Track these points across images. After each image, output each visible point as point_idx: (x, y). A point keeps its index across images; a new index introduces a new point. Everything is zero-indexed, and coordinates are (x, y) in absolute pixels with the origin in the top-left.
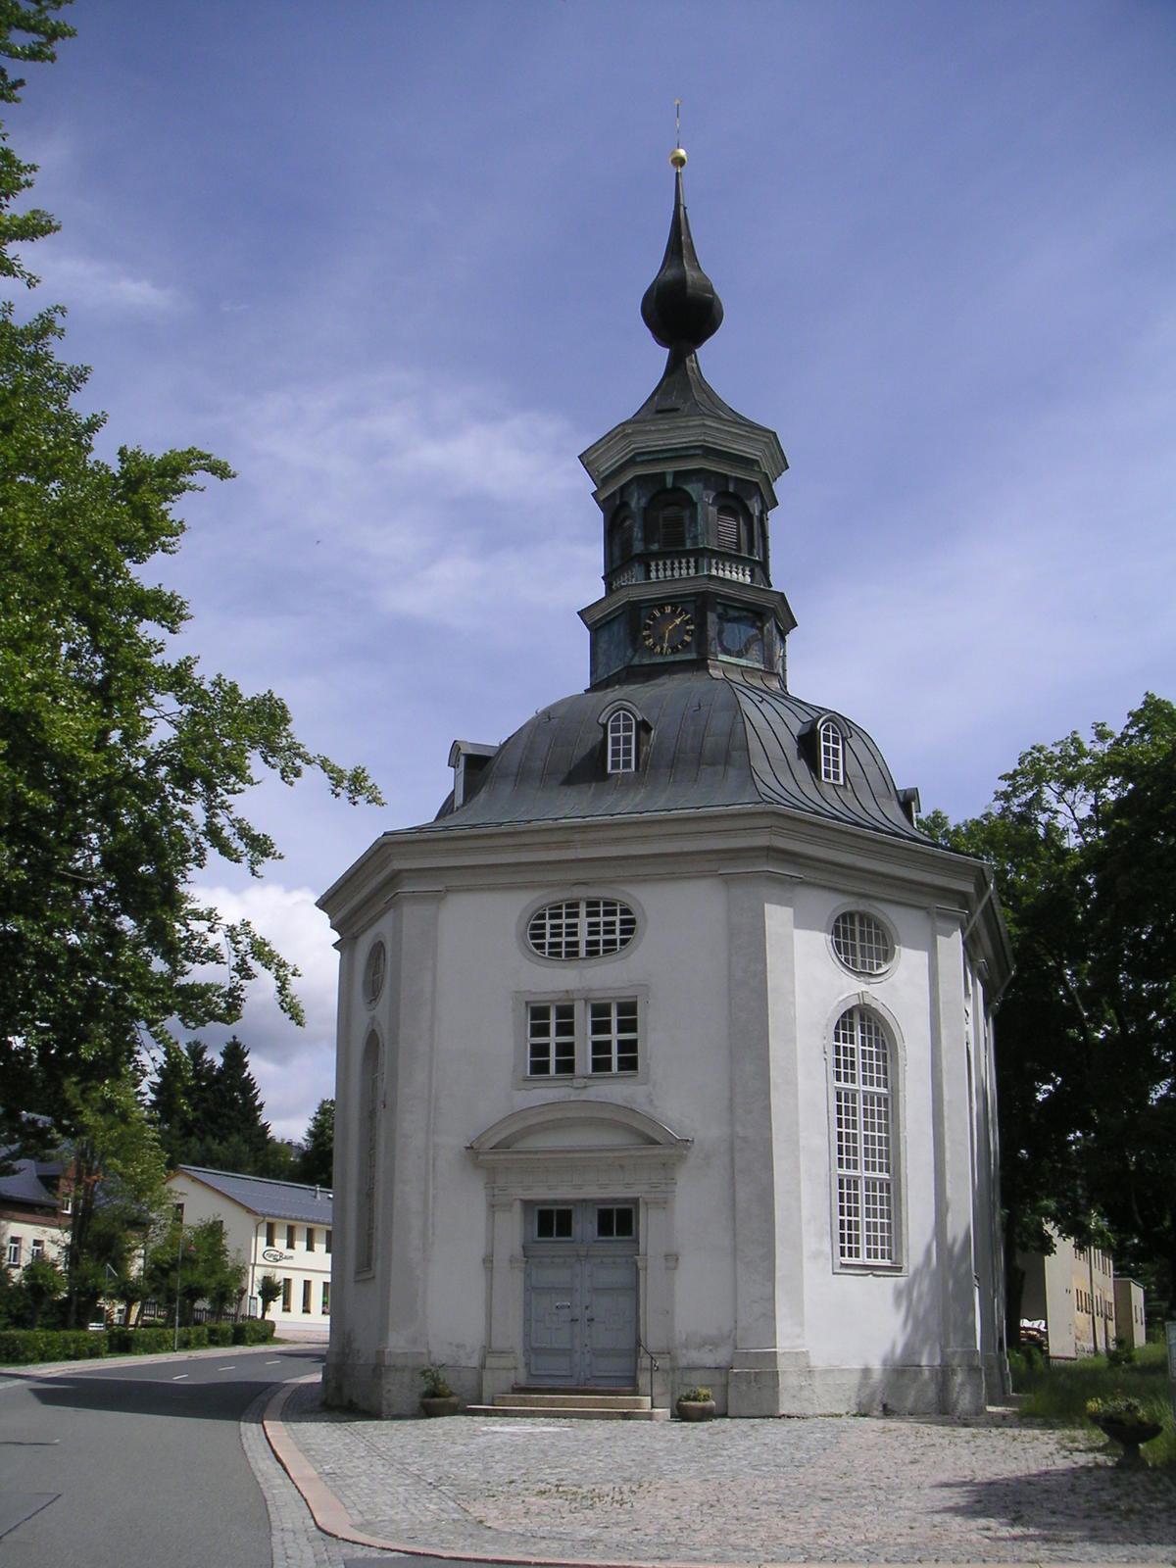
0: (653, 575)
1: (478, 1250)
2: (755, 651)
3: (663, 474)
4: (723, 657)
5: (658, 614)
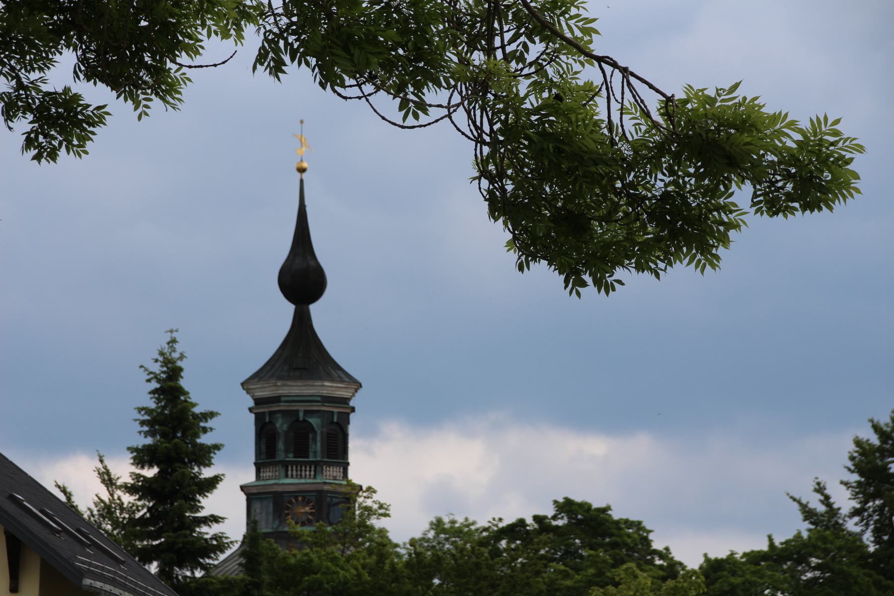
0: (290, 473)
3: (298, 411)
5: (294, 501)
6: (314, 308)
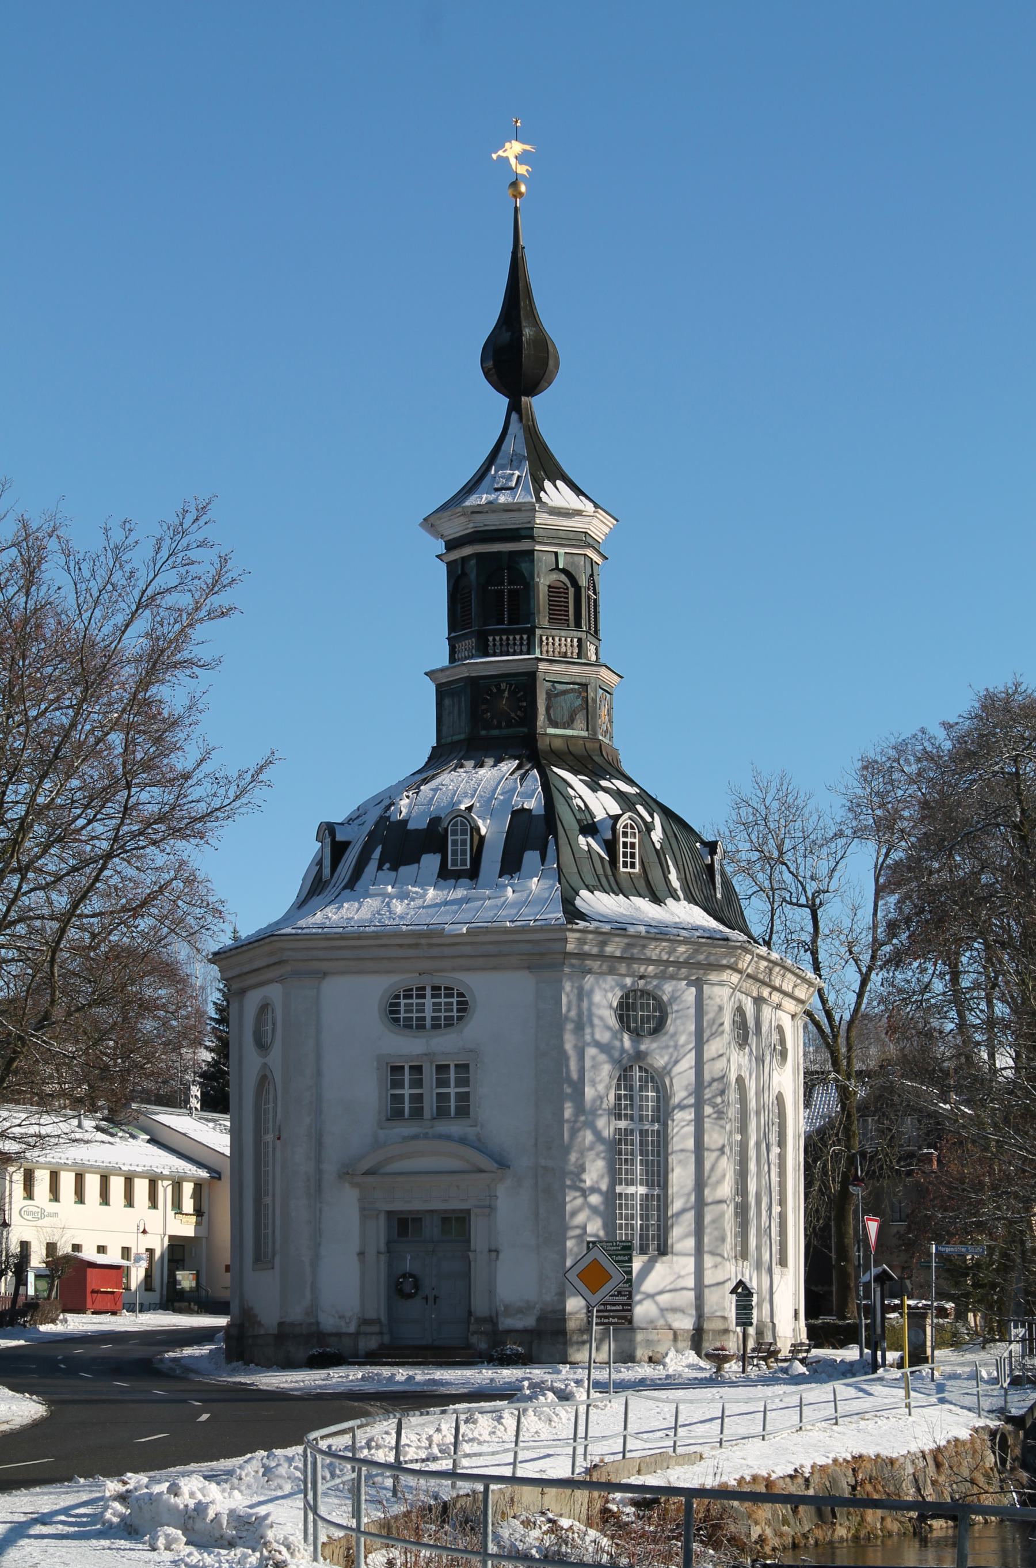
1: (355, 1246)
2: (580, 722)
4: (551, 731)
6: (538, 404)
